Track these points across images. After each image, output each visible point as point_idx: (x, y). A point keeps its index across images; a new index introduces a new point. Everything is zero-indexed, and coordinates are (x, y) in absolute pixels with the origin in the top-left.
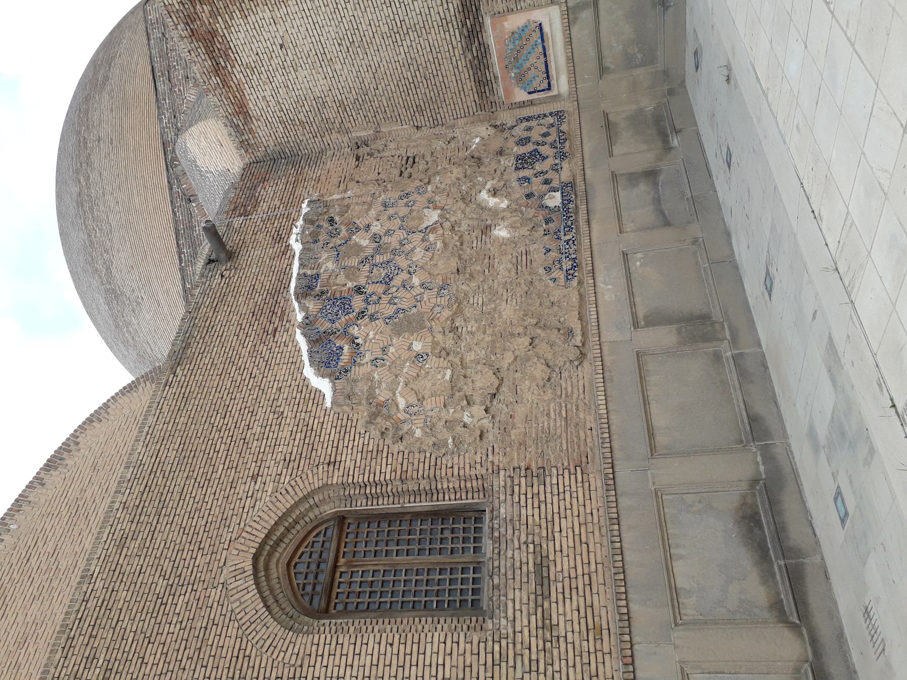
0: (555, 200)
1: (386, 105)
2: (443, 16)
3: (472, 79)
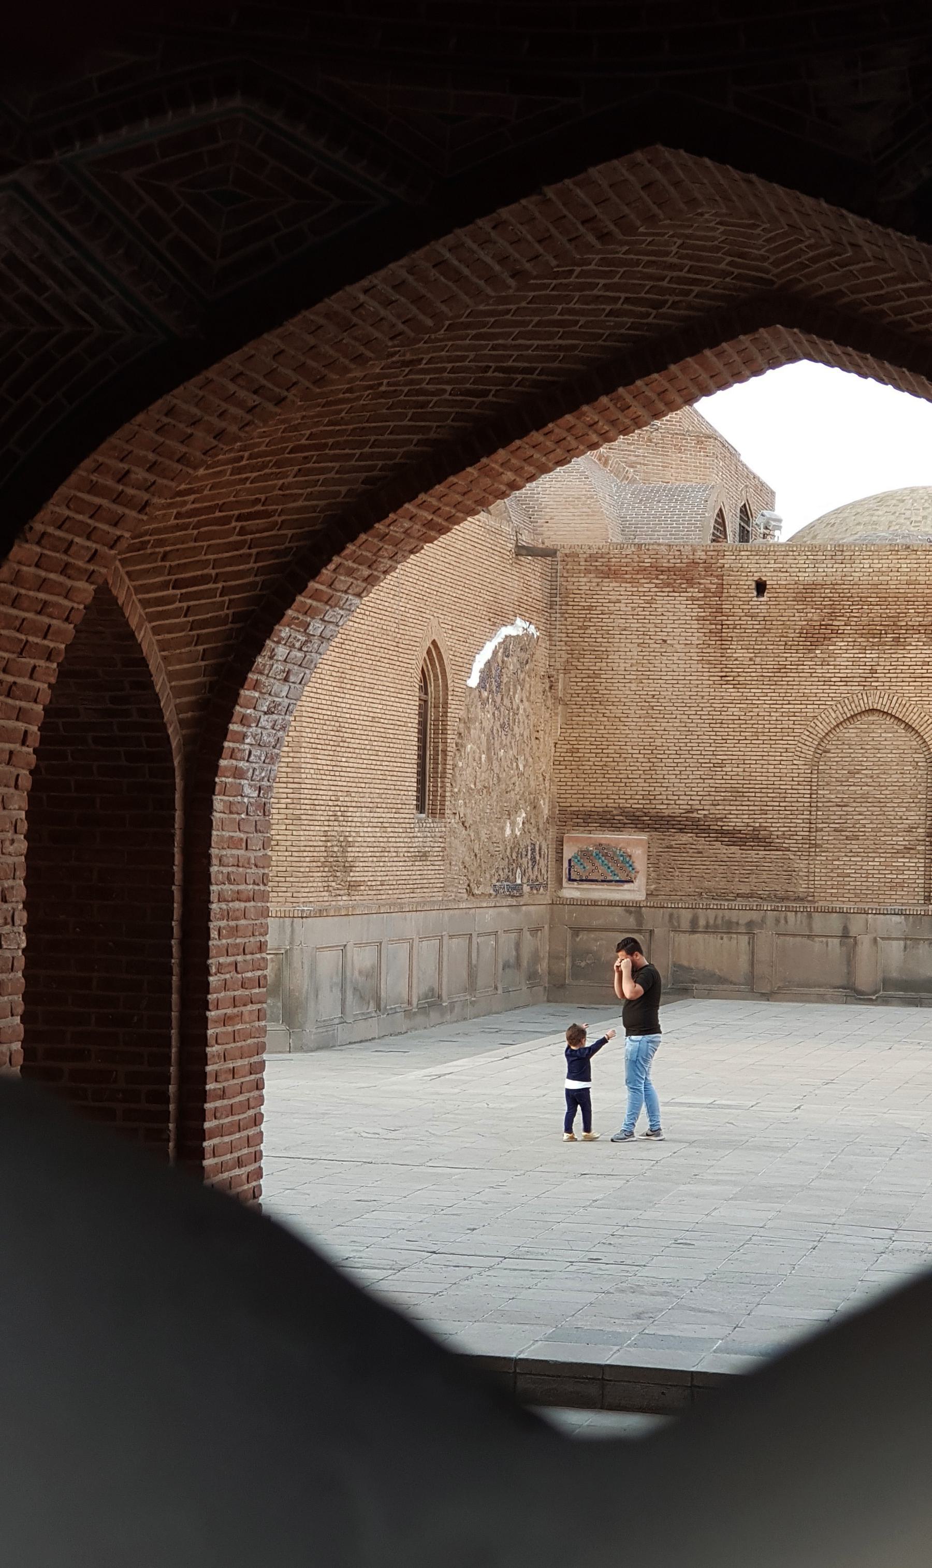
1: (586, 719)
2: (658, 797)
3: (593, 809)
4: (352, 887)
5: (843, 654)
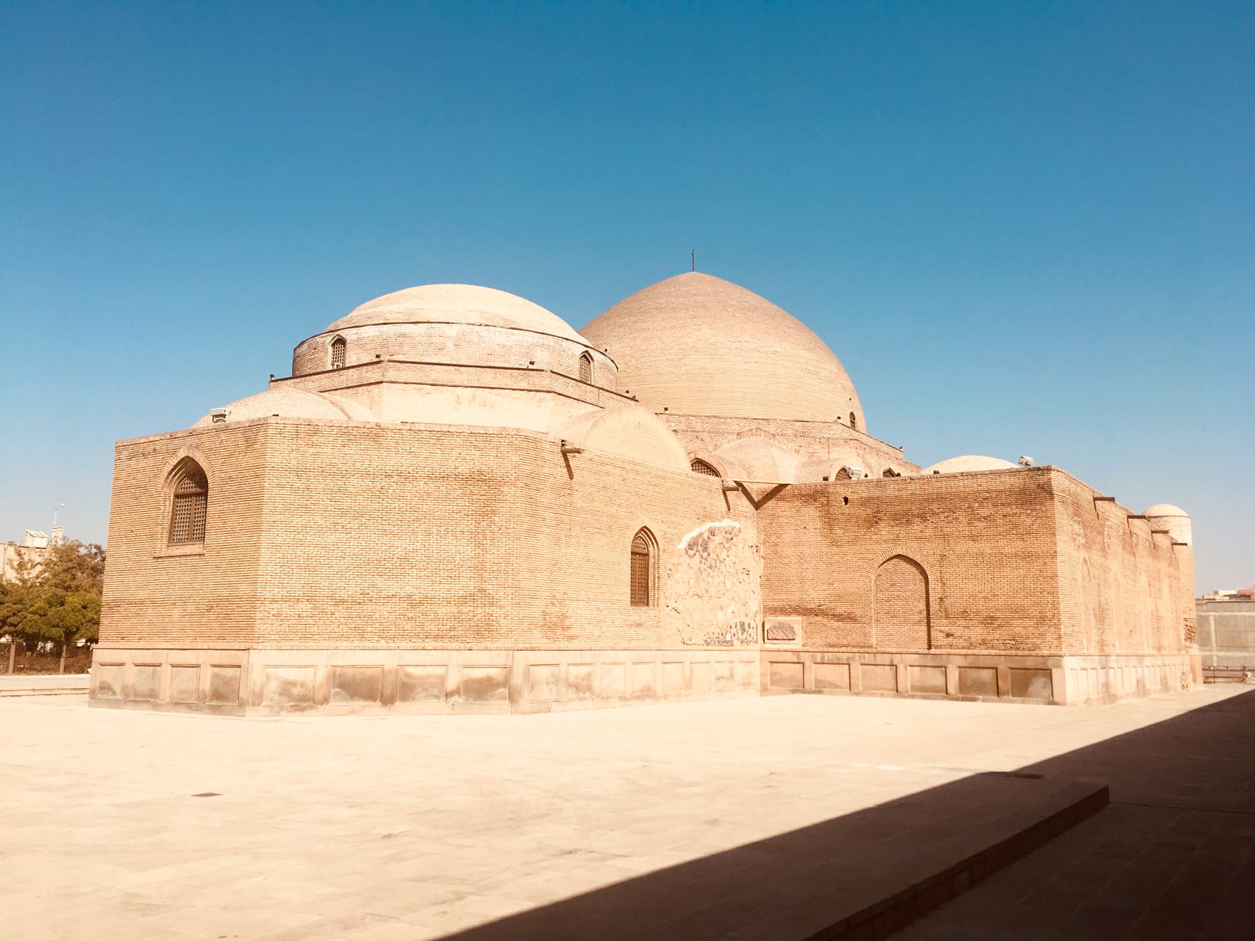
0: (728, 638)
4: (571, 638)
5: (885, 530)
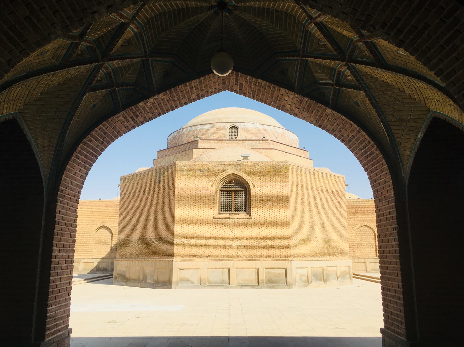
5: (360, 217)
